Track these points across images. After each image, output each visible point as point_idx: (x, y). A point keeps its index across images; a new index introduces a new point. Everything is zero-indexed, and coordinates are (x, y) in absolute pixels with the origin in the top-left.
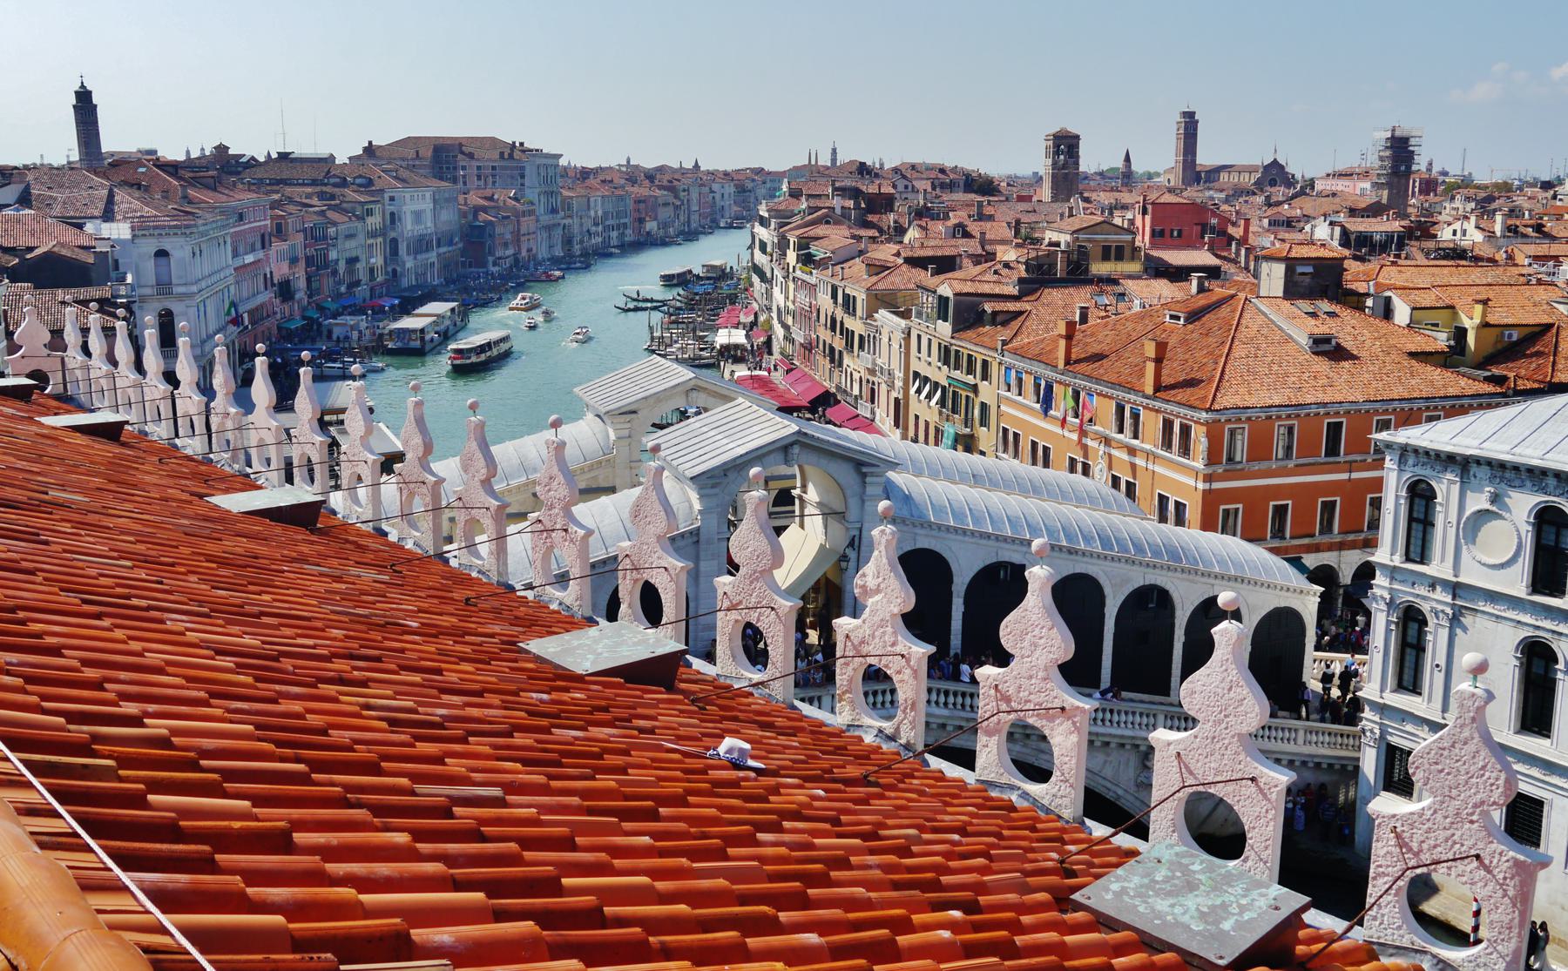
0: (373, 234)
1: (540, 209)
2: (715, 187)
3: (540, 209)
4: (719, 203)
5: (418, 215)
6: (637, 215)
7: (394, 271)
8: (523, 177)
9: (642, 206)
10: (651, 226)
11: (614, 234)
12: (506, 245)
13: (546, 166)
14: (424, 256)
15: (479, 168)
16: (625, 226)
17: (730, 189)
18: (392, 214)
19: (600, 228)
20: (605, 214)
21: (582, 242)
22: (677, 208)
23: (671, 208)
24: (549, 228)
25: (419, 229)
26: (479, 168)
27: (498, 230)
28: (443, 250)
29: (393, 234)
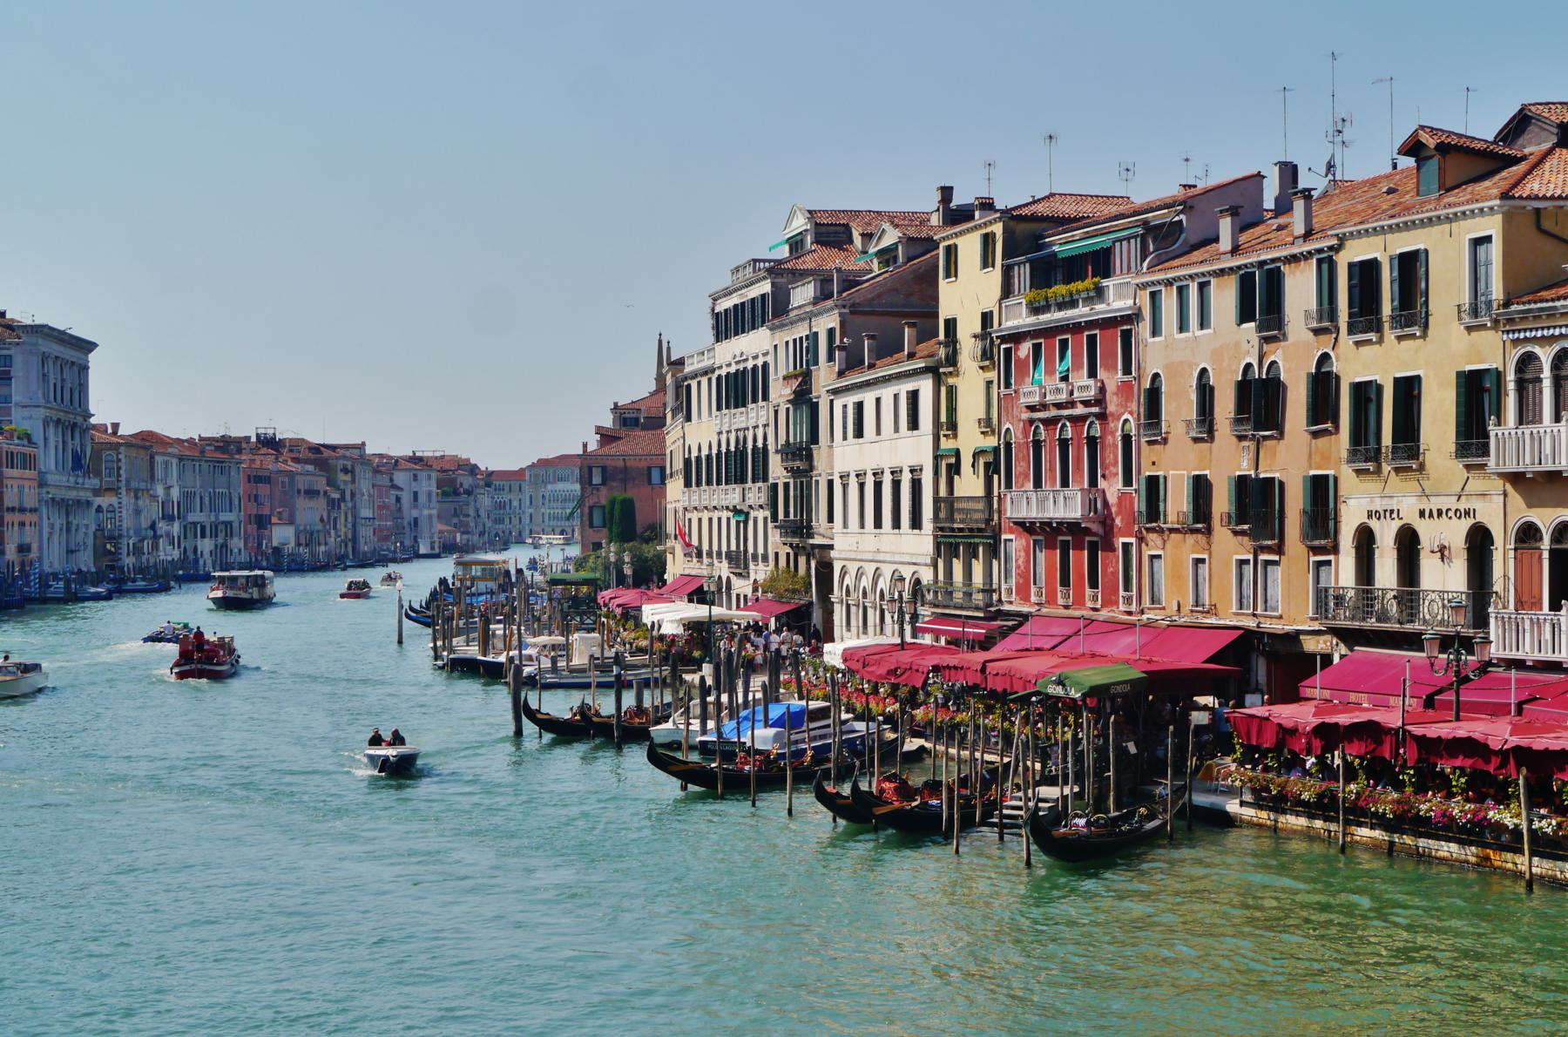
1: (48, 460)
2: (401, 478)
3: (48, 460)
4: (409, 513)
6: (253, 509)
9: (263, 489)
10: (282, 535)
11: (206, 545)
16: (228, 524)
19: (176, 528)
20: (187, 496)
21: (137, 551)
22: (333, 505)
23: (321, 503)
24: (68, 507)
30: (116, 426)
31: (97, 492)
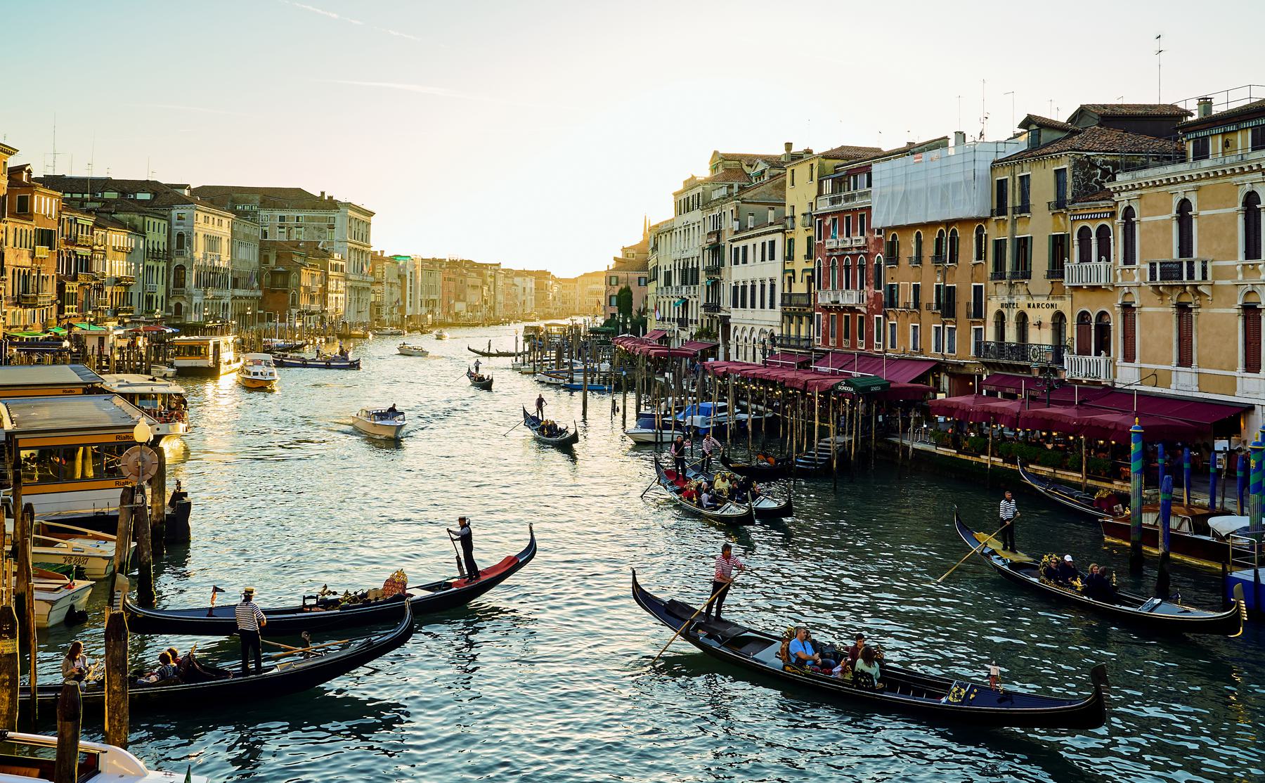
5: (212, 242)
7: (178, 306)
8: (332, 227)
10: (460, 307)
13: (359, 222)
16: (434, 301)
17: (530, 284)
18: (180, 236)
28: (238, 292)
29: (179, 261)
30: (382, 252)
31: (372, 284)
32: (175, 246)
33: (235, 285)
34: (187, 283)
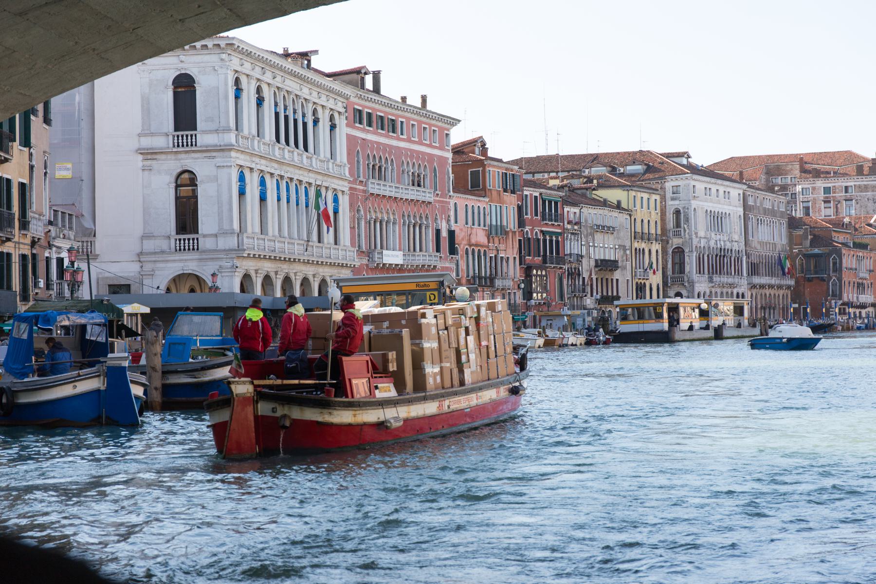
0: (645, 237)
5: (717, 220)
12: (860, 287)
14: (725, 279)
15: (827, 190)
18: (677, 212)
25: (718, 241)
26: (827, 190)
27: (848, 260)
28: (757, 280)
29: (676, 242)
32: (670, 224)
33: (754, 270)
34: (687, 269)
